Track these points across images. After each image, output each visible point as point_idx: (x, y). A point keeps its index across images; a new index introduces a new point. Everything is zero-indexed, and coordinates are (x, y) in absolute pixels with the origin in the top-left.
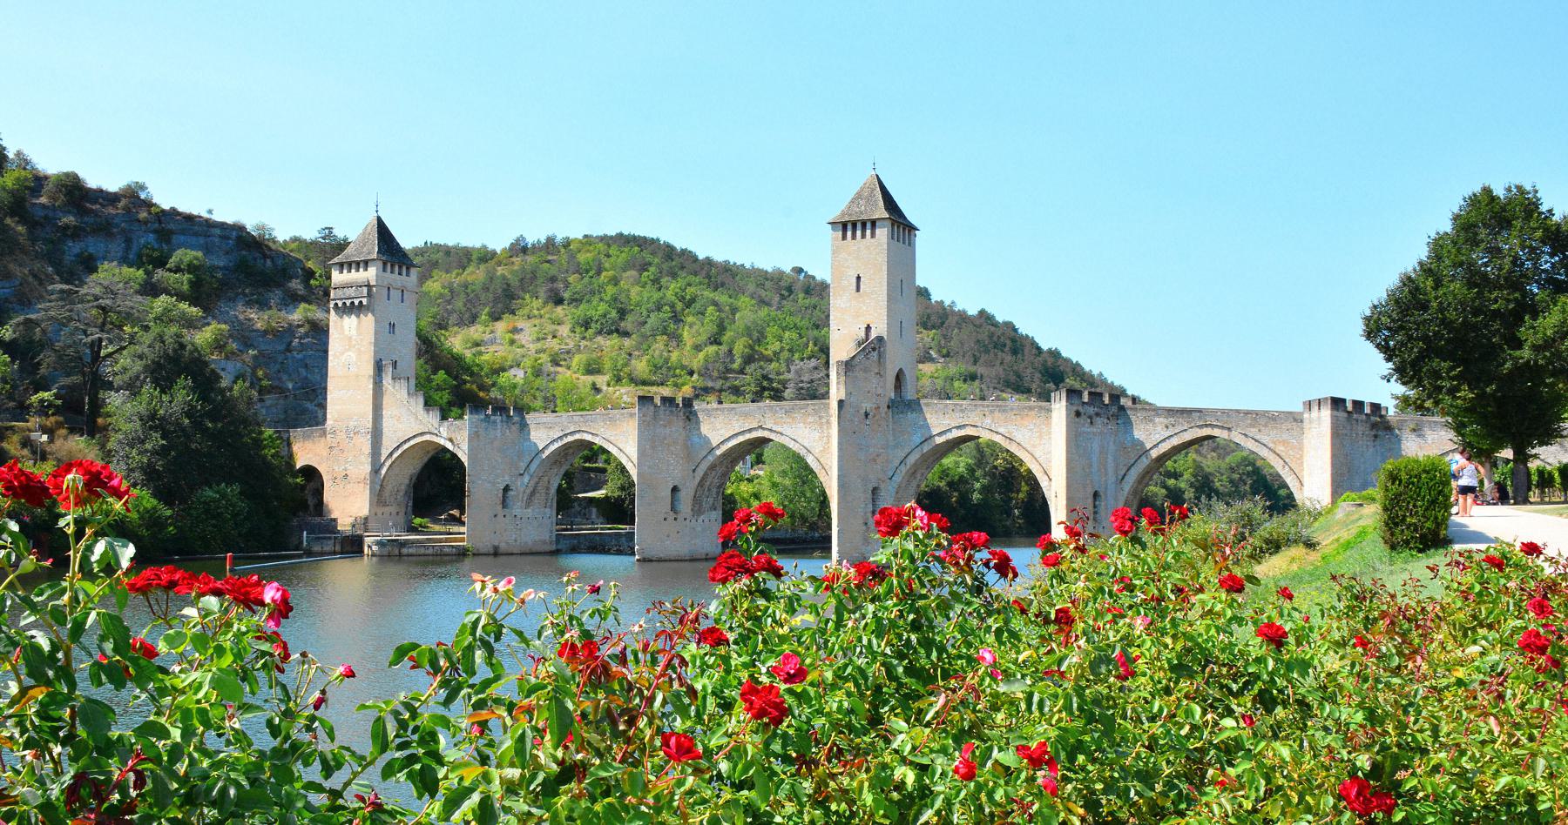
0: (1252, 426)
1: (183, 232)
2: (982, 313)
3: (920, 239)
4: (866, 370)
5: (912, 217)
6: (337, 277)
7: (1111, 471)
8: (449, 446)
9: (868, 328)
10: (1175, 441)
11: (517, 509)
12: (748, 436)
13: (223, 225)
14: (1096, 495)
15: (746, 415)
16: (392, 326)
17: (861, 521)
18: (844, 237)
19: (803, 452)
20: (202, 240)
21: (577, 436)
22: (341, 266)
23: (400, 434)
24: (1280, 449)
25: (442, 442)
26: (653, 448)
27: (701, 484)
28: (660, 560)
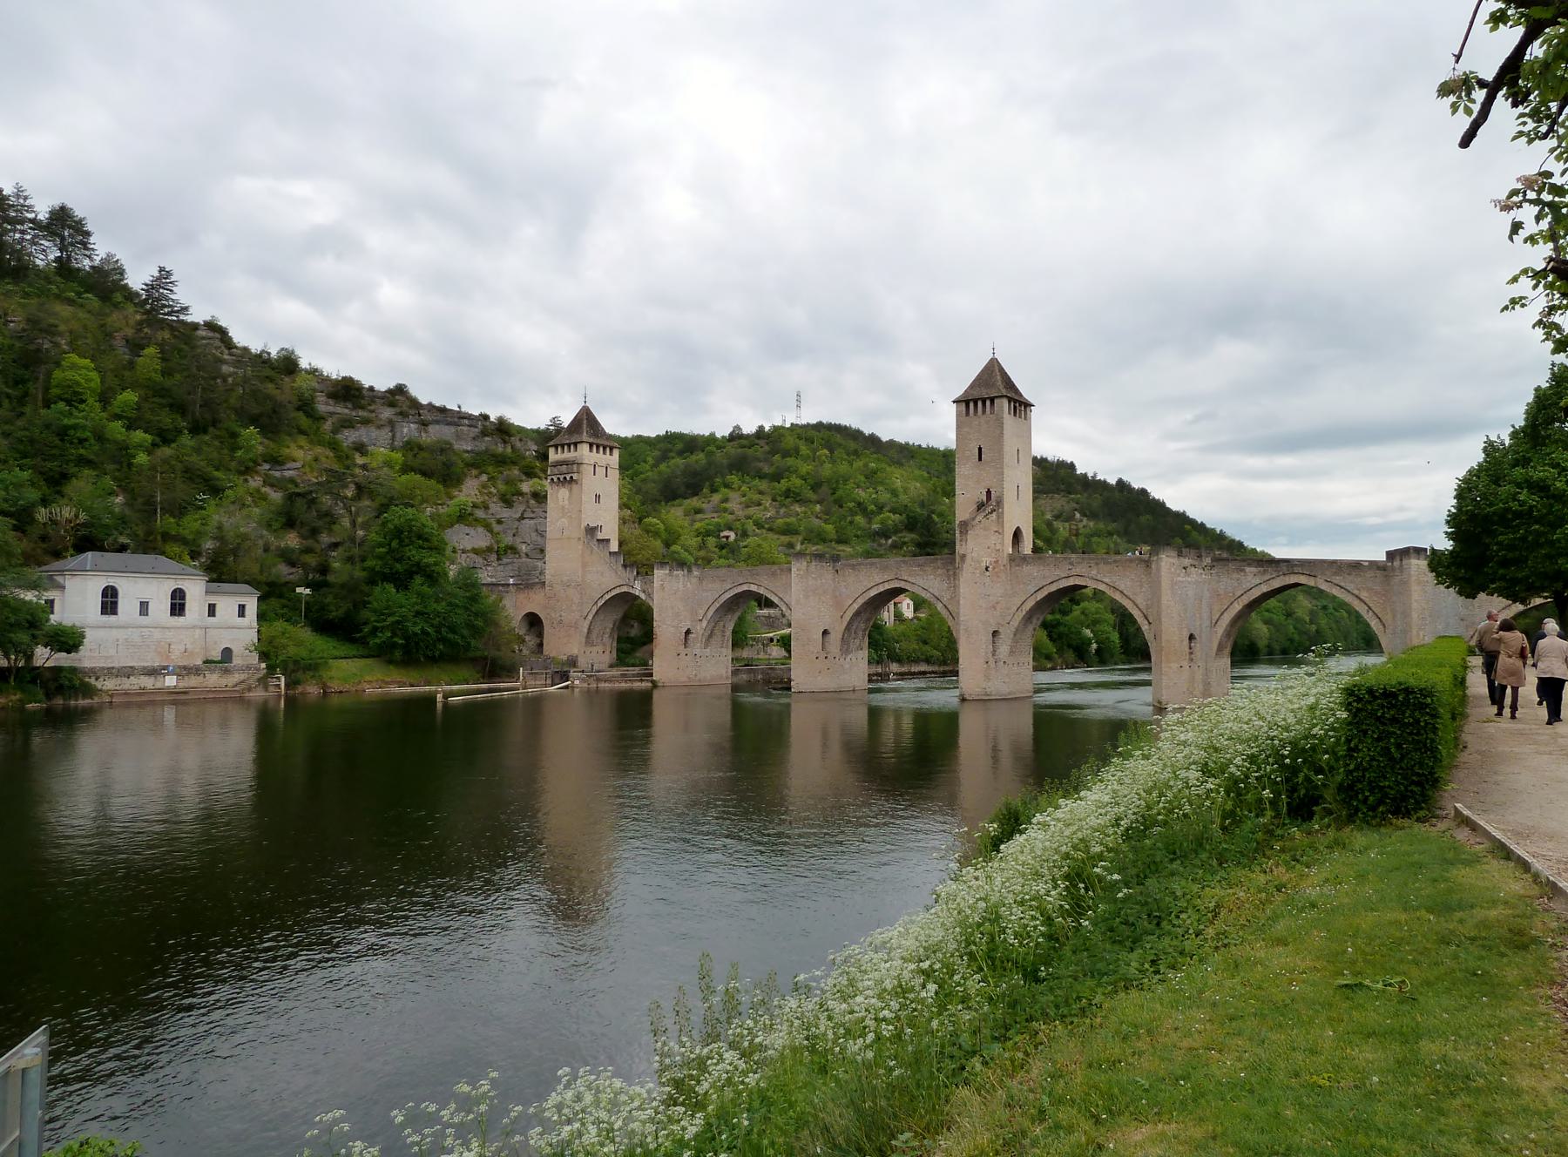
0: (1335, 574)
1: (437, 422)
3: (1035, 413)
5: (1027, 394)
6: (553, 456)
7: (1205, 616)
8: (643, 596)
9: (989, 492)
10: (1265, 589)
11: (697, 648)
13: (469, 417)
14: (1191, 637)
15: (885, 568)
16: (598, 497)
18: (968, 413)
19: (933, 600)
20: (453, 429)
21: (745, 588)
22: (556, 447)
24: (1364, 595)
26: (807, 597)
27: (848, 628)
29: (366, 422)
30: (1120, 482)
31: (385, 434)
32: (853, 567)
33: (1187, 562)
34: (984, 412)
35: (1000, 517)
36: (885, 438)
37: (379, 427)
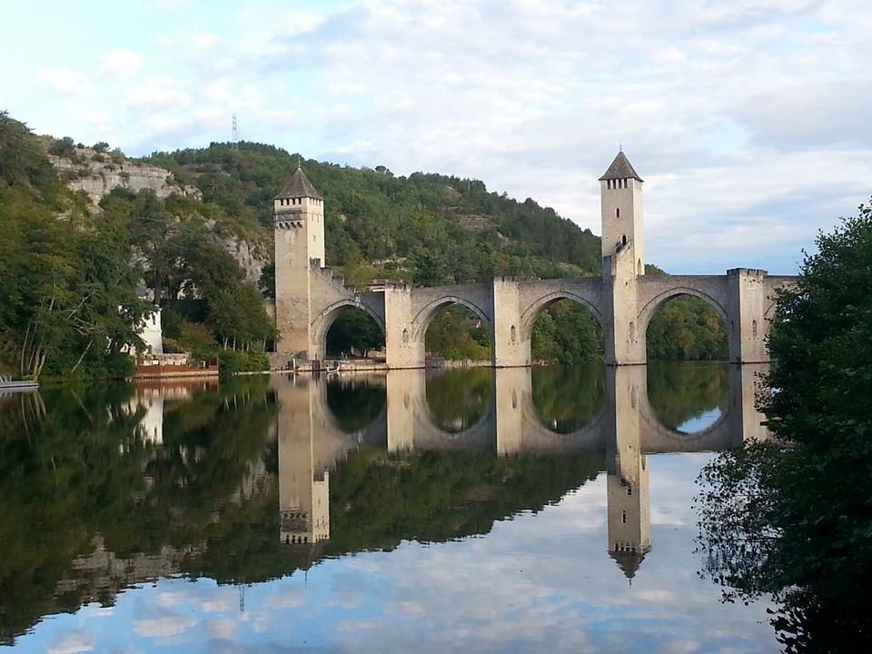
1: (135, 175)
2: (529, 200)
4: (625, 260)
8: (363, 308)
9: (624, 238)
12: (554, 297)
14: (754, 321)
15: (552, 285)
16: (315, 237)
17: (625, 341)
18: (609, 188)
19: (586, 304)
21: (448, 300)
23: (327, 301)
25: (358, 305)
28: (507, 367)
29: (83, 174)
30: (529, 200)
31: (99, 184)
32: (530, 284)
33: (752, 278)
34: (620, 187)
35: (633, 252)
36: (401, 170)
37: (95, 178)
